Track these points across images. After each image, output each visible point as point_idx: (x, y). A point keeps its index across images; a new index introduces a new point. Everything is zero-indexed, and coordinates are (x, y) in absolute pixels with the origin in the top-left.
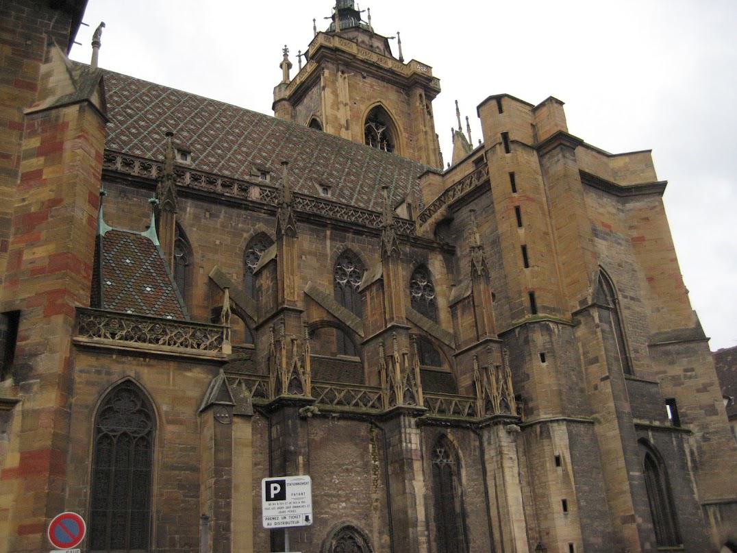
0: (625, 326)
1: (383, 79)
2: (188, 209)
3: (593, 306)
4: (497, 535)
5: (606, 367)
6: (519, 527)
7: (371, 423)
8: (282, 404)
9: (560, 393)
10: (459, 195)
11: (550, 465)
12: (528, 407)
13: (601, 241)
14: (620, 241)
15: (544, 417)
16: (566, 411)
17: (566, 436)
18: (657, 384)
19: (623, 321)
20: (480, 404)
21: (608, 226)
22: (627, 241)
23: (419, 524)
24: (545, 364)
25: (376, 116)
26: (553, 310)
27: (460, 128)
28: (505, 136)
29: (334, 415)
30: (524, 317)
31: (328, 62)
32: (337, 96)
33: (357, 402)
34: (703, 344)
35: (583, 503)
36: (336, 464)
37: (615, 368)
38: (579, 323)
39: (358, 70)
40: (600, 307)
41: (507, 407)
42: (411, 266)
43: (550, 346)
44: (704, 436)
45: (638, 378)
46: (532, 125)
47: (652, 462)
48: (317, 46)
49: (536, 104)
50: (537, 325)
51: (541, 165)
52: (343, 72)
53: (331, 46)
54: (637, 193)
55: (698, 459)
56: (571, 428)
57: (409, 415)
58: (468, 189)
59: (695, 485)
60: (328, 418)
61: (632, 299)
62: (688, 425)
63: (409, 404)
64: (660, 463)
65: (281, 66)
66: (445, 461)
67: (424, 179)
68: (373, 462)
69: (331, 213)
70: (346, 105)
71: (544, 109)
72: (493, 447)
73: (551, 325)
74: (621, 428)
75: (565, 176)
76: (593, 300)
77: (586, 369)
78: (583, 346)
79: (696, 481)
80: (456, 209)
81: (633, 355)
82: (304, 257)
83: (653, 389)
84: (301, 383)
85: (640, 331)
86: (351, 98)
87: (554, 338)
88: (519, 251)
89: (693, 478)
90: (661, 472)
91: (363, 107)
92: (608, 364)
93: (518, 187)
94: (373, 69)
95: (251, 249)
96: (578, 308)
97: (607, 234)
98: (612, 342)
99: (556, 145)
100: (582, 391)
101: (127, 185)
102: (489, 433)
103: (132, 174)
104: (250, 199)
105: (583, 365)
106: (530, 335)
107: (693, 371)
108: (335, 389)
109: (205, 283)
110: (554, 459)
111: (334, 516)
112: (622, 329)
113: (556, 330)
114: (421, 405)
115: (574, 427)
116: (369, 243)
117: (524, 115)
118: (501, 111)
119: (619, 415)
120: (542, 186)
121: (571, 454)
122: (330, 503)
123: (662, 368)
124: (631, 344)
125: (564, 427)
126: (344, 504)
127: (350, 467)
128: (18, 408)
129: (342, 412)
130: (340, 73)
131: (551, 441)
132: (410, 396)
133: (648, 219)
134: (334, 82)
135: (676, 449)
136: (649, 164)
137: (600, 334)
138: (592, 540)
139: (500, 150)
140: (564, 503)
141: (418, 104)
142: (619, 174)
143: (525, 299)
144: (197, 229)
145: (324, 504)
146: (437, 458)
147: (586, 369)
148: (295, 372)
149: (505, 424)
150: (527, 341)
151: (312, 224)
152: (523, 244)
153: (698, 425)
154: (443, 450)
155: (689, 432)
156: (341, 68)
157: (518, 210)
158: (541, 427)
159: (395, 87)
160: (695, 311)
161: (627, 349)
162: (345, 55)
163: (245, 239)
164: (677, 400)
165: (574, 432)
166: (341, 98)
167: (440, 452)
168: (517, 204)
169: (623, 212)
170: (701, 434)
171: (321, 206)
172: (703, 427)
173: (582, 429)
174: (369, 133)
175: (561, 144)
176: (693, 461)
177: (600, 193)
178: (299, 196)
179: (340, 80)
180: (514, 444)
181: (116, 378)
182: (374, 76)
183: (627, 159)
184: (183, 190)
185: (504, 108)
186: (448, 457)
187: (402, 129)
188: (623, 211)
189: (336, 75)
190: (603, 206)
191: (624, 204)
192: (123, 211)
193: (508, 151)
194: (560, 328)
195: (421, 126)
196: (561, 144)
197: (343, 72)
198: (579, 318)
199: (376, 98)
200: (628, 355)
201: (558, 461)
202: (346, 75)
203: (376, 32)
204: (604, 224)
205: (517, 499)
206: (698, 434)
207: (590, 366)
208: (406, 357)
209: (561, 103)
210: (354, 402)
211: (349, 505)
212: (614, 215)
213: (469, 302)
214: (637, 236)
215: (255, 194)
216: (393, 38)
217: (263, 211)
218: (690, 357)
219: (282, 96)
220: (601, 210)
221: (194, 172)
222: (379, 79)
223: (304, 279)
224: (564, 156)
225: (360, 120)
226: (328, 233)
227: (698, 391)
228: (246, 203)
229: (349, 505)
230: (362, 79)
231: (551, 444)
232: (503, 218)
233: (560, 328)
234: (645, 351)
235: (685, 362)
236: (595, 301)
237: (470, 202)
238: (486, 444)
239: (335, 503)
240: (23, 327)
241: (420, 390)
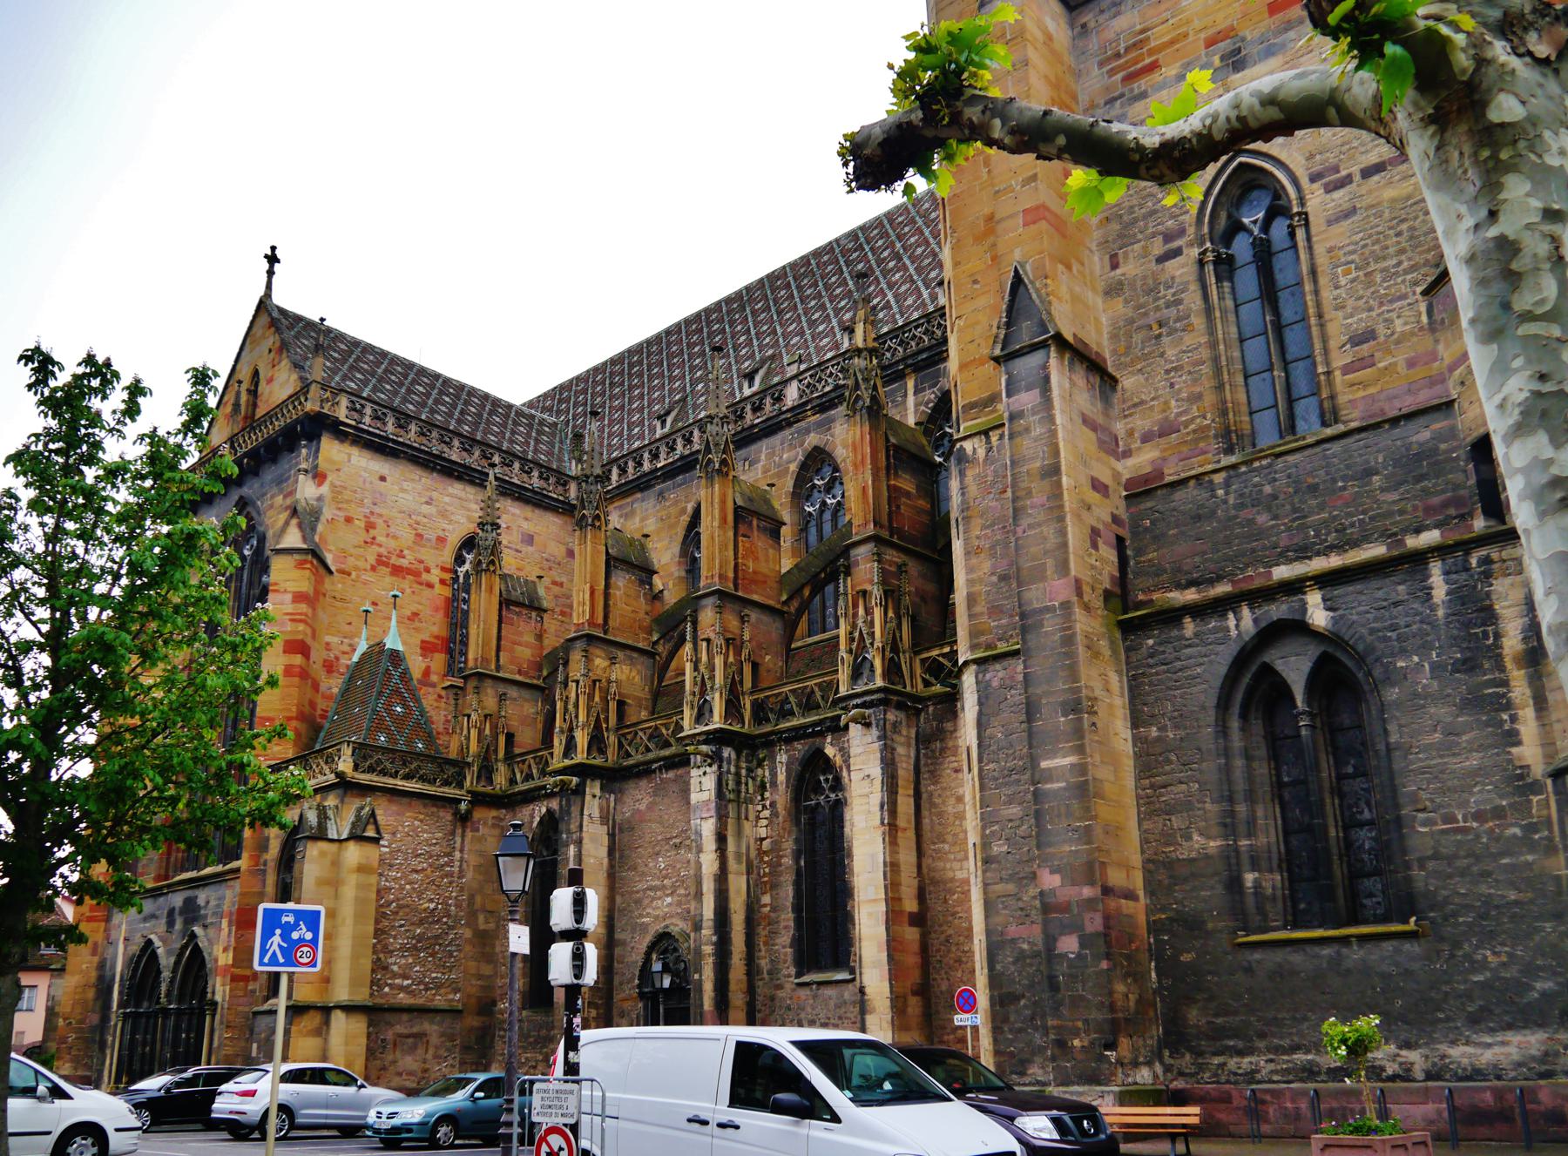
6: (870, 914)
16: (983, 639)
23: (704, 924)
35: (999, 848)
45: (1354, 425)
59: (1528, 714)
98: (1038, 431)
103: (659, 465)
111: (657, 917)
122: (653, 899)
126: (669, 900)
127: (677, 841)
129: (664, 758)
132: (702, 714)
138: (1013, 930)
145: (646, 902)
154: (831, 777)
165: (995, 683)
167: (827, 780)
205: (873, 856)
211: (676, 898)
215: (792, 394)
228: (783, 417)
229: (676, 898)
239: (660, 898)
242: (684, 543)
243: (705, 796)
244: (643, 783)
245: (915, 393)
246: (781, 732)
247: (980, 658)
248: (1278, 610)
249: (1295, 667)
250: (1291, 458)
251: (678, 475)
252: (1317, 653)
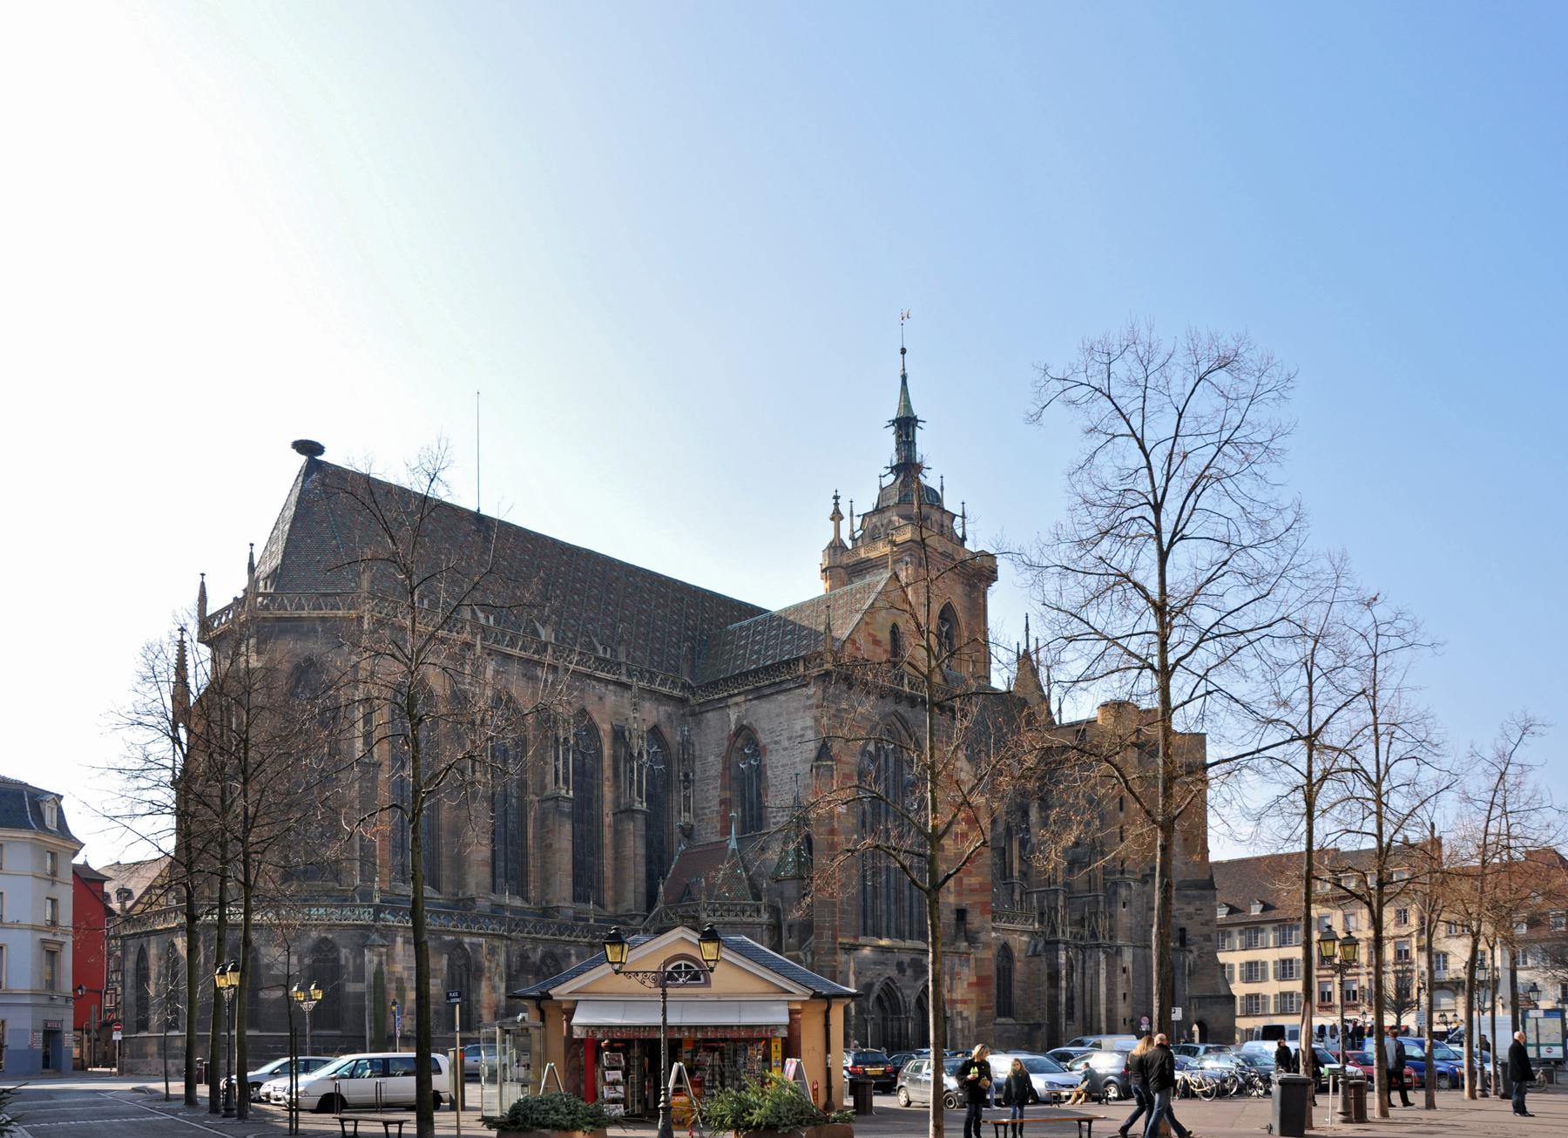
4: (1088, 1011)
9: (1131, 928)
11: (1119, 971)
15: (1119, 942)
27: (1028, 646)
123: (1182, 906)
128: (972, 956)
140: (1125, 994)
172: (1201, 948)
176: (1189, 970)
181: (1002, 942)
201: (1124, 970)
227: (1202, 924)
240: (969, 918)
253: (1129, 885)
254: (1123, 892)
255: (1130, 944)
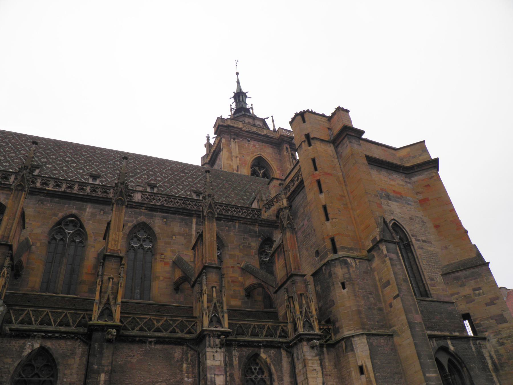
0: (420, 261)
1: (262, 141)
2: (88, 210)
3: (381, 241)
5: (396, 288)
7: (188, 346)
8: (93, 329)
9: (359, 312)
10: (293, 188)
11: (355, 373)
12: (335, 327)
13: (394, 203)
14: (409, 203)
15: (346, 333)
17: (367, 347)
18: (453, 303)
19: (417, 258)
20: (290, 326)
21: (400, 193)
22: (415, 202)
24: (345, 291)
25: (258, 163)
26: (351, 249)
28: (307, 136)
29: (150, 340)
30: (328, 257)
31: (224, 134)
32: (231, 152)
33: (174, 329)
34: (484, 268)
36: (149, 382)
37: (404, 287)
38: (373, 256)
39: (244, 137)
40: (387, 241)
41: (311, 327)
42: (260, 239)
43: (349, 276)
44: (498, 341)
45: (435, 300)
46: (329, 128)
47: (455, 367)
48: (217, 126)
49: (328, 114)
50: (337, 262)
51: (337, 152)
52: (234, 139)
53: (225, 124)
54: (419, 169)
55: (497, 361)
56: (371, 341)
57: (214, 336)
58: (296, 183)
60: (145, 343)
61: (424, 241)
62: (484, 333)
63: (216, 327)
64: (462, 368)
65: (205, 146)
66: (260, 376)
67: (271, 184)
68: (186, 379)
69: (195, 207)
70: (237, 157)
71: (335, 116)
72: (300, 361)
73: (349, 260)
74: (413, 335)
75: (352, 154)
76: (380, 236)
77: (382, 292)
78: (378, 274)
79: (499, 381)
80: (293, 198)
81: (429, 282)
82: (174, 237)
83: (450, 308)
84: (112, 312)
85: (433, 264)
86: (240, 153)
87: (351, 270)
88: (322, 211)
89: (495, 379)
90: (465, 374)
91: (248, 158)
92: (397, 285)
93: (318, 167)
94: (255, 136)
95: (134, 234)
96: (371, 245)
97: (398, 198)
98: (399, 267)
99: (344, 135)
100: (380, 310)
101: (44, 196)
102: (297, 350)
103: (47, 188)
104: (134, 201)
105: (380, 289)
106: (332, 269)
107: (481, 289)
108: (154, 319)
109: (95, 258)
110: (358, 370)
112: (418, 263)
113: (354, 264)
114: (226, 327)
115: (375, 341)
116: (226, 226)
117: (322, 123)
118: (304, 121)
119: (411, 326)
120: (338, 165)
121: (372, 362)
124: (427, 274)
125: (364, 340)
130: (232, 140)
131: (354, 353)
132: (216, 320)
133: (430, 186)
134: (229, 145)
135: (475, 354)
136: (425, 150)
137: (388, 262)
139: (305, 145)
141: (285, 153)
142: (404, 160)
143: (328, 244)
144: (93, 222)
146: (253, 375)
147: (382, 292)
148: (108, 302)
149: (309, 340)
150: (330, 275)
151: (181, 215)
152: (324, 204)
153: (492, 333)
154: (258, 368)
155: (484, 339)
156: (233, 136)
157: (319, 182)
158: (345, 342)
159: (270, 145)
160: (475, 245)
161: (423, 278)
162: (235, 129)
163: (129, 227)
164: (471, 314)
165: (374, 344)
166: (233, 154)
167: (255, 369)
168: (318, 178)
169: (411, 184)
170: (496, 340)
171: (188, 203)
172: (497, 333)
173: (382, 341)
174: (254, 173)
175: (347, 134)
176: (494, 364)
177: (391, 172)
178: (171, 197)
179: (232, 143)
180: (318, 358)
182: (256, 140)
183: (408, 149)
184: (85, 197)
185: (306, 119)
186: (263, 373)
187: (276, 169)
188: (410, 183)
189: (230, 141)
190: (393, 180)
191: (410, 178)
192: (39, 212)
193: (310, 145)
194: (357, 262)
195: (288, 165)
196: (347, 134)
197: (234, 139)
198: (373, 253)
199: (258, 152)
200: (425, 282)
201: (361, 370)
202: (236, 140)
203: (258, 116)
204: (394, 192)
206: (494, 341)
207: (385, 289)
208: (214, 289)
209: (347, 111)
210: (171, 329)
212: (403, 185)
213: (281, 250)
214: (422, 198)
216: (267, 118)
217: (144, 208)
218: (477, 278)
219: (205, 162)
220: (392, 183)
221: (93, 186)
222: (259, 141)
223: (173, 252)
224: (350, 142)
225: (247, 166)
226: (194, 220)
227: (487, 304)
230: (247, 142)
231: (354, 356)
232: (310, 189)
233: (357, 262)
234: (440, 279)
235: (473, 283)
236: (382, 237)
237: (300, 192)
238: (296, 360)
241: (226, 316)
242: (52, 229)
243: (217, 363)
244: (135, 347)
245: (196, 224)
246: (239, 341)
247: (368, 333)
248: (442, 343)
249: (444, 360)
250: (425, 303)
251: (56, 197)
252: (448, 358)
253: (346, 263)
254: (339, 271)
255: (360, 332)
